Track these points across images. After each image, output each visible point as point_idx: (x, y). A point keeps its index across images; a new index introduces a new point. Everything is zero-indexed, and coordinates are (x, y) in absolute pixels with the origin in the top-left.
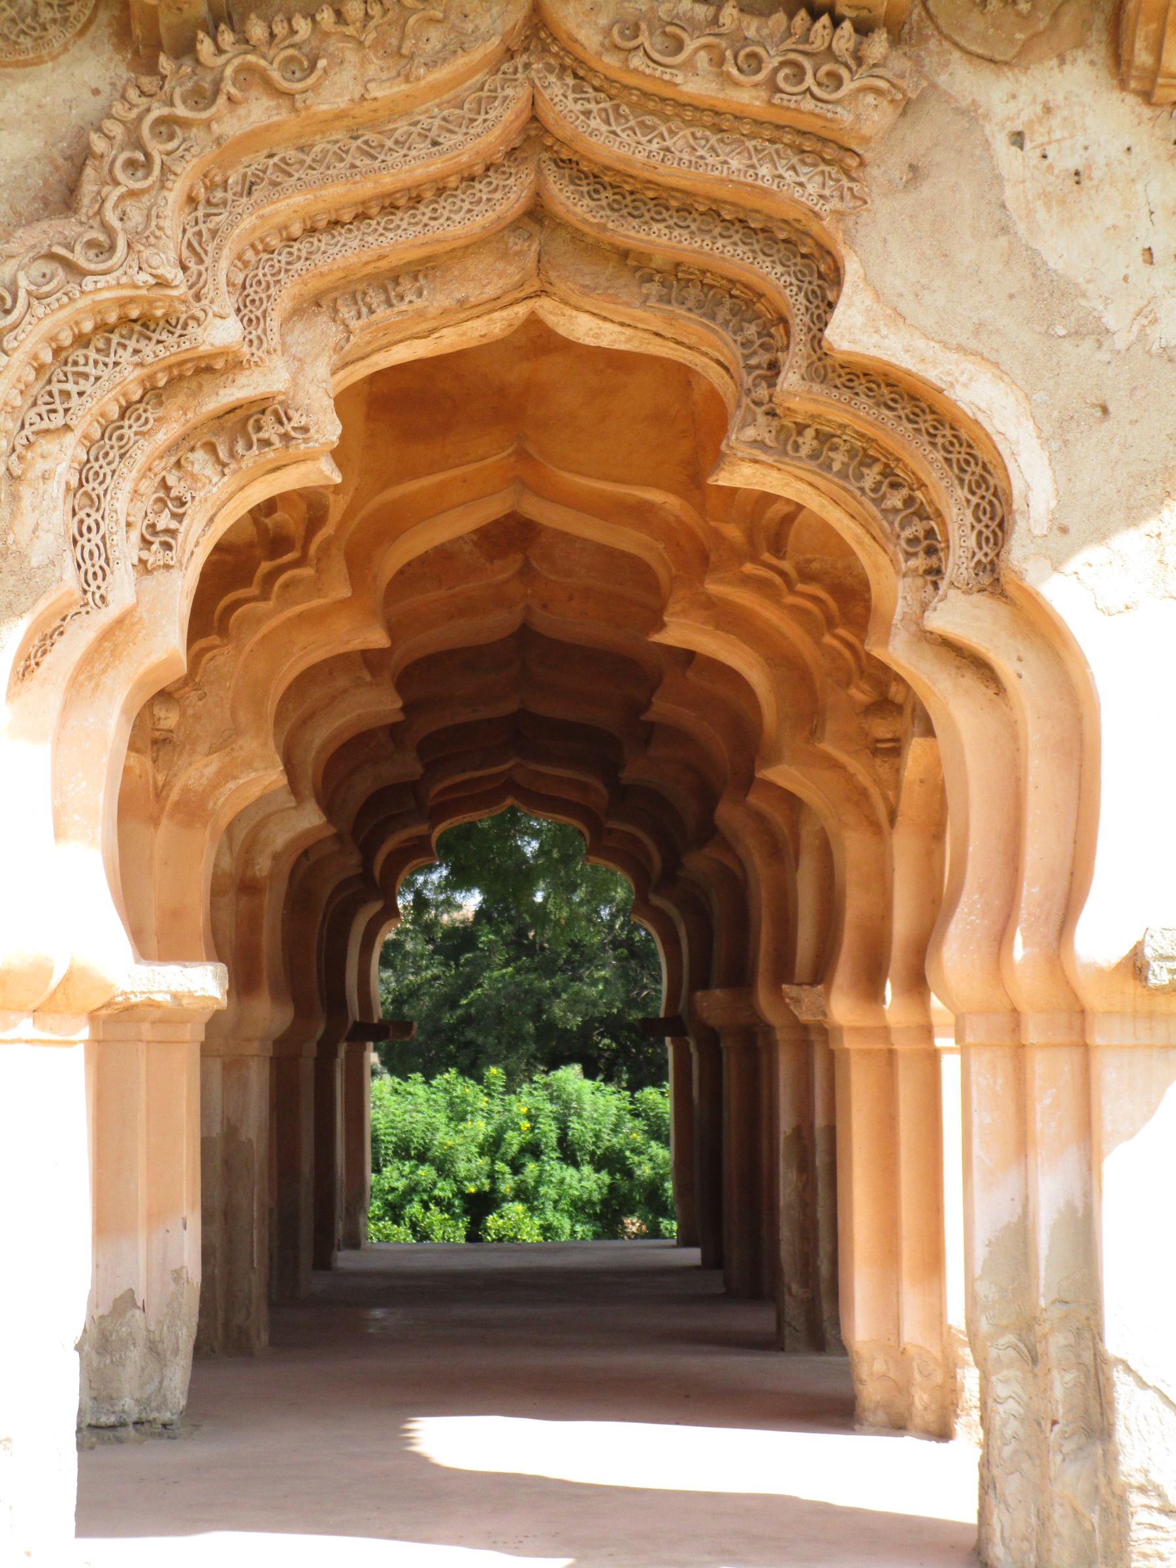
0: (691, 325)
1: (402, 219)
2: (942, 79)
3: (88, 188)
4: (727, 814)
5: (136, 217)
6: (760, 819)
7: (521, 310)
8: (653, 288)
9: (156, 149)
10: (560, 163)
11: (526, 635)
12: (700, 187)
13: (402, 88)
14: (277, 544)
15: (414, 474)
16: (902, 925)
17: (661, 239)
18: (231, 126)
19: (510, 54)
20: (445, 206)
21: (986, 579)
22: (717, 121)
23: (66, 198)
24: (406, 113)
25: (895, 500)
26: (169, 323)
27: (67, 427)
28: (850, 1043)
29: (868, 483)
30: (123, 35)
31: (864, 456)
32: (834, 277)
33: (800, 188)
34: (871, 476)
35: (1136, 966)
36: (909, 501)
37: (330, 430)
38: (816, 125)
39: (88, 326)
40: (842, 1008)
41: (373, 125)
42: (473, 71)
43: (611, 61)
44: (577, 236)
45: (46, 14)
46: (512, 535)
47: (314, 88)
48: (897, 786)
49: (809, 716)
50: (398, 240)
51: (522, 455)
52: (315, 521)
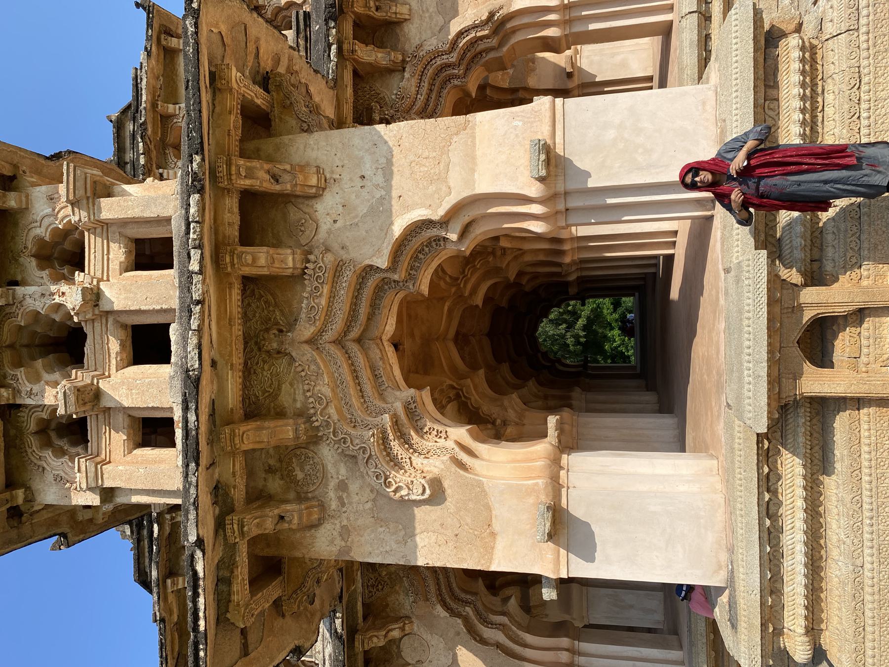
0: (386, 302)
1: (360, 374)
2: (321, 241)
3: (351, 453)
4: (527, 289)
5: (357, 441)
6: (528, 281)
7: (386, 344)
8: (377, 312)
9: (341, 436)
10: (345, 335)
11: (489, 335)
12: (350, 301)
13: (325, 376)
14: (458, 396)
15: (442, 364)
17: (363, 310)
18: (335, 417)
19: (318, 348)
20: (357, 364)
21: (444, 226)
22: (332, 297)
24: (333, 374)
25: (427, 249)
26: (384, 432)
27: (410, 458)
28: (576, 258)
29: (423, 257)
31: (415, 258)
32: (371, 266)
33: (348, 277)
34: (421, 256)
35: (541, 179)
36: (427, 246)
37: (412, 391)
38: (332, 272)
39: (385, 453)
40: (567, 260)
41: (335, 382)
42: (321, 358)
43: (318, 323)
44: (364, 331)
45: (311, 462)
46: (461, 339)
47: (326, 397)
48: (512, 249)
49: (498, 270)
50: (365, 375)
51: (437, 339)
52: (454, 388)
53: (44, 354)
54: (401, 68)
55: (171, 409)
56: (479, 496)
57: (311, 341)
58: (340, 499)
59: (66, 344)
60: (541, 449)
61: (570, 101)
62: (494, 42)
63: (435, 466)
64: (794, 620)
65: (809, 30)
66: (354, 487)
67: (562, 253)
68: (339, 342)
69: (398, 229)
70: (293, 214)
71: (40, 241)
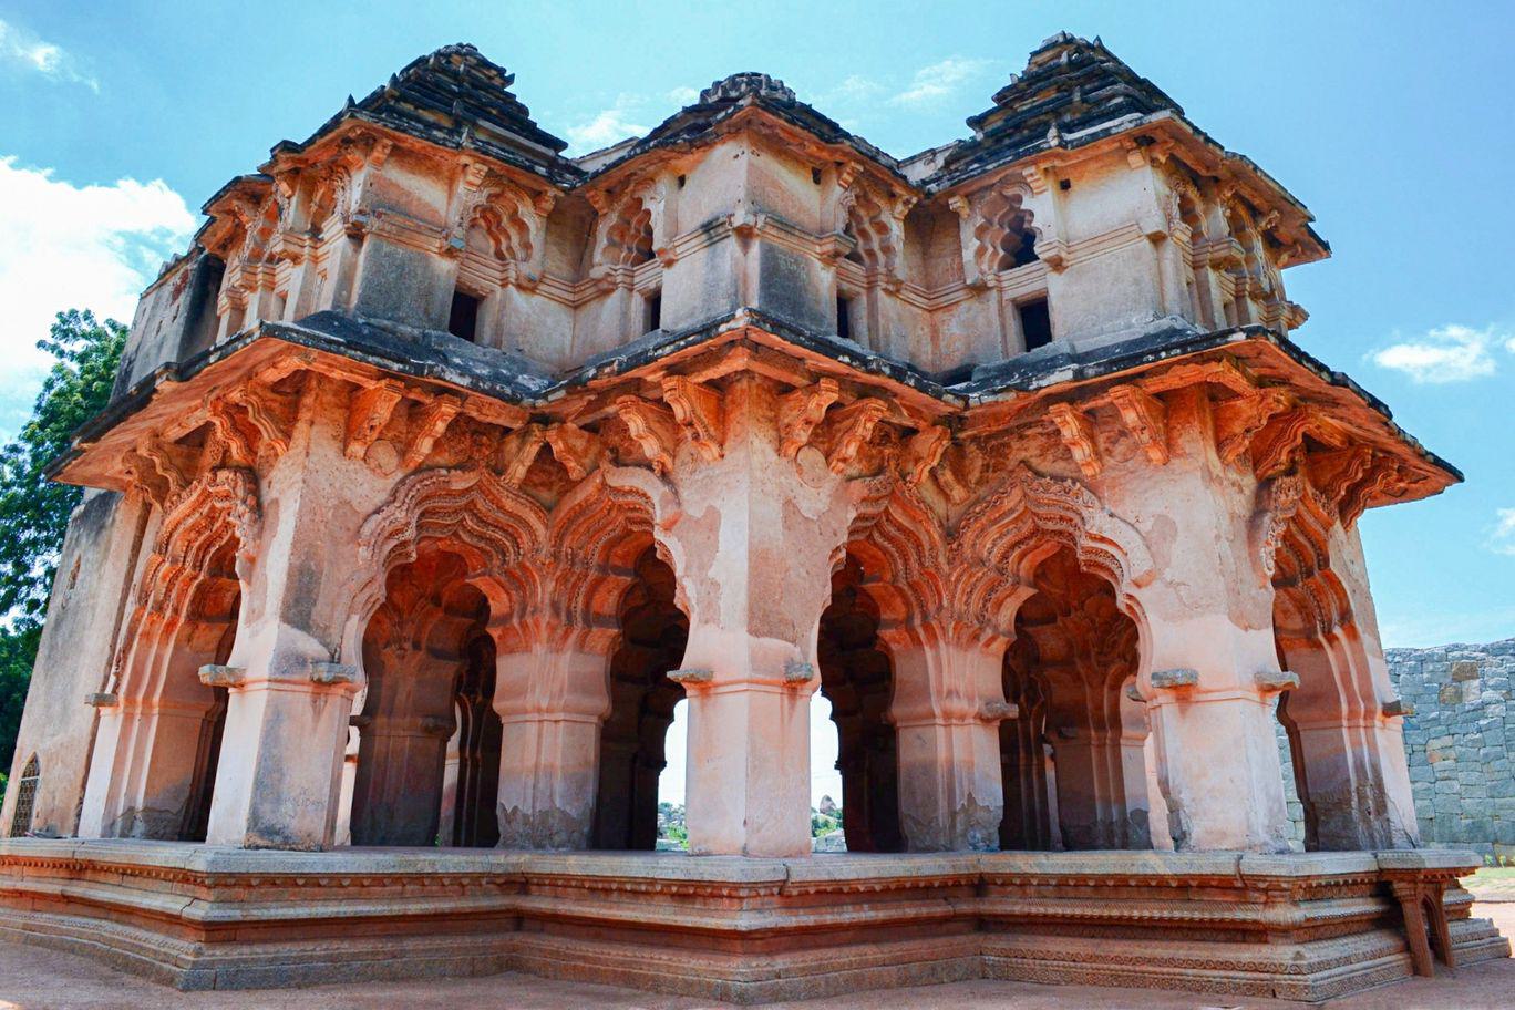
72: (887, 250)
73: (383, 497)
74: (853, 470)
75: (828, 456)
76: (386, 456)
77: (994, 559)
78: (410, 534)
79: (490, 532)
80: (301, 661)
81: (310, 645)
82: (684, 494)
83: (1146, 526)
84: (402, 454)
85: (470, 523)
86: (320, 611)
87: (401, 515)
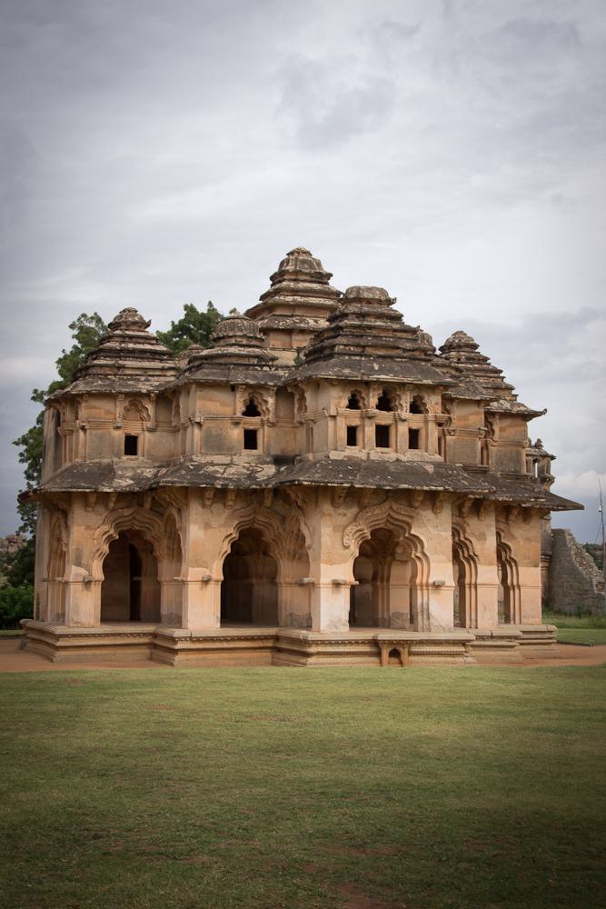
16: (386, 575)
23: (355, 519)
30: (358, 506)
33: (410, 520)
35: (434, 583)
53: (384, 393)
54: (461, 514)
55: (364, 448)
56: (345, 561)
57: (391, 508)
58: (340, 514)
59: (385, 404)
60: (351, 579)
61: (452, 592)
62: (466, 555)
63: (352, 547)
64: (321, 649)
65: (466, 654)
66: (345, 518)
67: (382, 581)
68: (389, 514)
69: (422, 538)
70: (428, 503)
71: (422, 398)
72: (267, 409)
73: (102, 522)
74: (238, 507)
75: (225, 505)
76: (100, 509)
77: (295, 532)
78: (112, 532)
79: (143, 525)
80: (80, 575)
81: (83, 571)
82: (183, 520)
83: (311, 529)
84: (106, 506)
85: (136, 523)
86: (84, 561)
87: (106, 528)
